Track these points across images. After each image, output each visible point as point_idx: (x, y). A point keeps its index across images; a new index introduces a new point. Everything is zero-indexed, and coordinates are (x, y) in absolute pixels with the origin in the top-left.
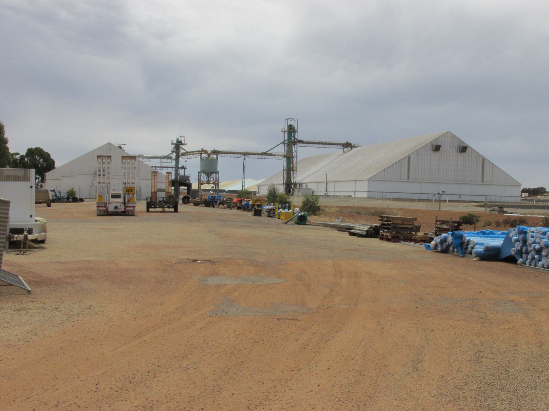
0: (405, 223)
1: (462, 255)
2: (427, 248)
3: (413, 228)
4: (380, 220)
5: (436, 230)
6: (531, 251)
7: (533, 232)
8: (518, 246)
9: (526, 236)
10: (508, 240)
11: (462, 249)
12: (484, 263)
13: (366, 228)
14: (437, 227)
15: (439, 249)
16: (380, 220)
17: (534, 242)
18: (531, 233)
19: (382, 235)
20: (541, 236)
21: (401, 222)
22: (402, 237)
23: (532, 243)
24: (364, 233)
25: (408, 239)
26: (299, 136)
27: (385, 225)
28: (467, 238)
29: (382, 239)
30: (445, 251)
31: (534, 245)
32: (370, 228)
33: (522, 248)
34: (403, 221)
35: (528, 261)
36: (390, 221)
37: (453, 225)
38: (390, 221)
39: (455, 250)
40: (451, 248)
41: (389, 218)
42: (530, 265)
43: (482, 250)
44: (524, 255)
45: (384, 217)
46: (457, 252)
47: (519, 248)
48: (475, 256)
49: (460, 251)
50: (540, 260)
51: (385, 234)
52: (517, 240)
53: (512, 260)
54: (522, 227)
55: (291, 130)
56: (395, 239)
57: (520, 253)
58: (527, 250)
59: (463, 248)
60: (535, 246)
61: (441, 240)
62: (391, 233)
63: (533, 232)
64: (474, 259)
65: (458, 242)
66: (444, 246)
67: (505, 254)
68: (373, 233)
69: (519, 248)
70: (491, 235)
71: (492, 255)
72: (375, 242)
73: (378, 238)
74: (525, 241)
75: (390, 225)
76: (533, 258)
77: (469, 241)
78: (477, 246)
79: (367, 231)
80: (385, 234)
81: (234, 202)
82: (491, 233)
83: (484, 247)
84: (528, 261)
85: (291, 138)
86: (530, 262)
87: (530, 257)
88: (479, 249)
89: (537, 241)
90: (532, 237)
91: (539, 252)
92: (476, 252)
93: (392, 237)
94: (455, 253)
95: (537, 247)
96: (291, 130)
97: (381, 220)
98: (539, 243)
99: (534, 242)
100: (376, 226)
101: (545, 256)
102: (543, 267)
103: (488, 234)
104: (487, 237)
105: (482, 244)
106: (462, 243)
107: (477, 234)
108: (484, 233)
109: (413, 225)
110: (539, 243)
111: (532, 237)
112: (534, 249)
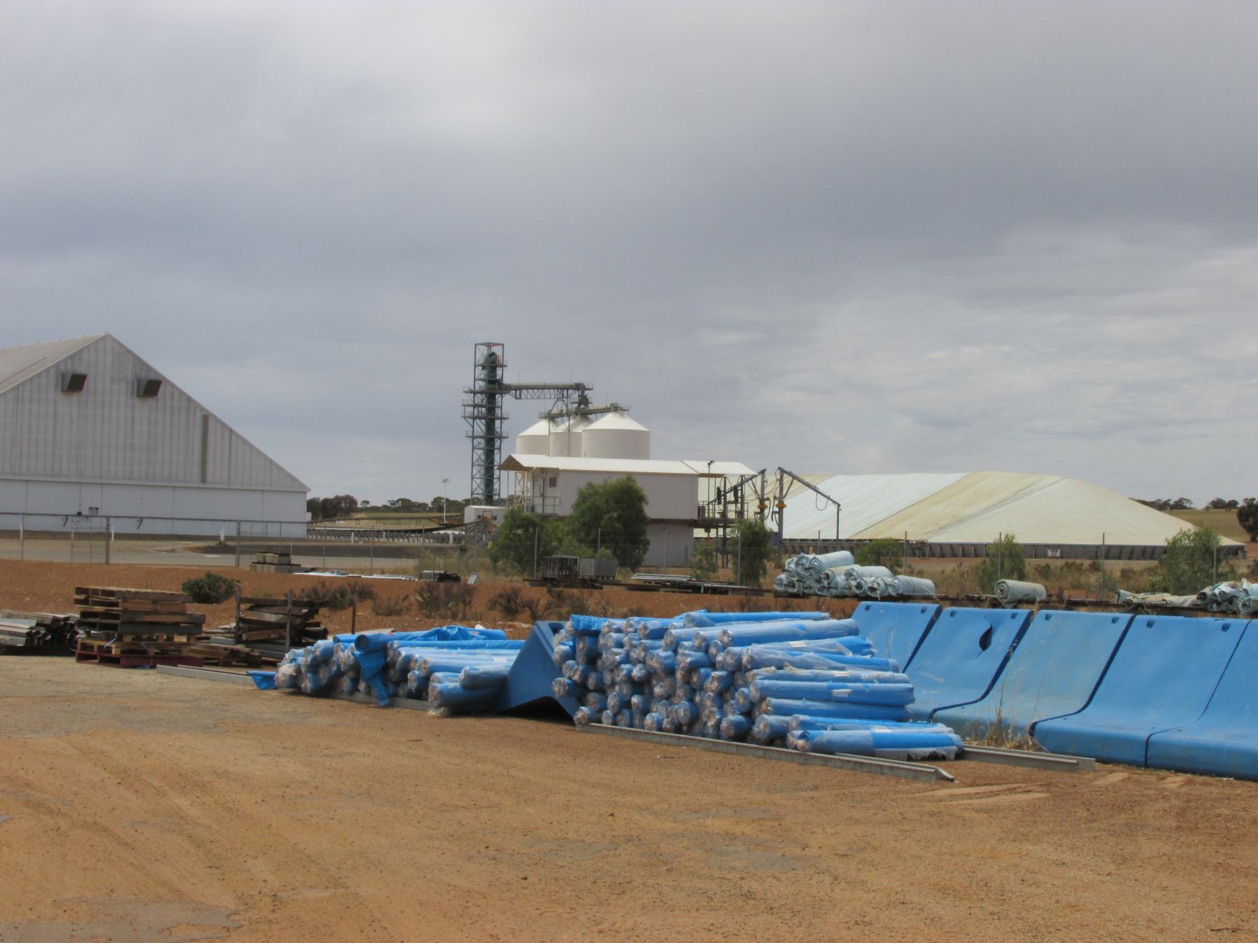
0: (159, 607)
1: (386, 701)
2: (259, 684)
3: (178, 624)
4: (78, 602)
5: (237, 628)
6: (613, 684)
7: (619, 631)
8: (573, 671)
9: (597, 642)
10: (534, 654)
11: (385, 685)
12: (468, 722)
13: (24, 626)
14: (241, 620)
15: (307, 684)
16: (78, 602)
17: (627, 659)
18: (614, 635)
19: (84, 646)
20: (648, 642)
21: (149, 607)
22: (152, 651)
23: (620, 663)
24: (20, 642)
25: (171, 657)
26: (508, 376)
27: (96, 615)
28: (404, 652)
29: (83, 658)
30: (326, 691)
31: (628, 666)
32: (38, 625)
33: (585, 677)
34: (155, 602)
35: (609, 713)
36: (116, 604)
37: (295, 611)
38: (116, 604)
39: (362, 686)
40: (346, 683)
41: (112, 593)
42: (615, 723)
43: (457, 684)
44: (592, 697)
45: (95, 592)
46: (369, 692)
47: (576, 677)
48: (436, 703)
49: (378, 687)
50: (645, 711)
51: (96, 643)
52: (571, 655)
53: (548, 711)
54: (584, 620)
55: (492, 364)
56: (134, 658)
57: (579, 692)
58: (600, 681)
59: (386, 680)
60: (630, 671)
61: (314, 659)
62: (120, 639)
63: (619, 631)
64: (432, 712)
65: (369, 665)
66: (324, 676)
67: (525, 693)
68: (51, 640)
69: (576, 677)
70: (464, 642)
71: (483, 700)
72: (64, 666)
73: (71, 654)
74: (593, 659)
75: (116, 617)
76: (626, 704)
77: (408, 659)
78: (438, 675)
79: (28, 634)
80: (96, 643)
81: (422, 596)
82: (463, 635)
83: (462, 675)
84: (609, 713)
85: (493, 387)
86: (615, 715)
87: (612, 700)
88: (447, 683)
89: (634, 655)
90: (620, 645)
91: (641, 686)
92: (441, 693)
93: (122, 652)
94: (360, 696)
95: (637, 672)
96: (492, 364)
97: (85, 602)
98: (644, 662)
99: (627, 659)
100: (56, 620)
101: (661, 698)
102: (660, 729)
103: (455, 638)
104: (455, 647)
105: (456, 670)
106: (386, 667)
107: (426, 637)
108: (443, 636)
109: (183, 614)
110: (644, 662)
111: (620, 645)
112: (629, 678)
